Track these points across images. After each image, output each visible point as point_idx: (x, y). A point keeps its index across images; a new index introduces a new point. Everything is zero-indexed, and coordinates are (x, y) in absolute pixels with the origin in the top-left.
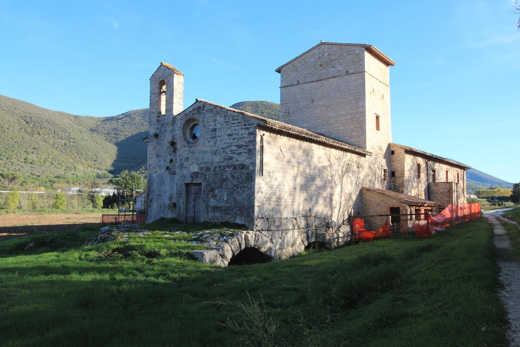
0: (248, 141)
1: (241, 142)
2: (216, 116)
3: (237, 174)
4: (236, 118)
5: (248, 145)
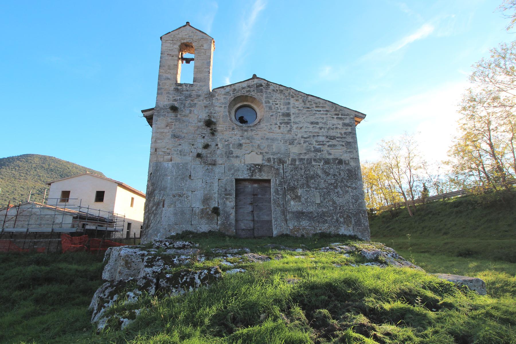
0: (343, 132)
1: (332, 133)
2: (289, 99)
5: (344, 138)
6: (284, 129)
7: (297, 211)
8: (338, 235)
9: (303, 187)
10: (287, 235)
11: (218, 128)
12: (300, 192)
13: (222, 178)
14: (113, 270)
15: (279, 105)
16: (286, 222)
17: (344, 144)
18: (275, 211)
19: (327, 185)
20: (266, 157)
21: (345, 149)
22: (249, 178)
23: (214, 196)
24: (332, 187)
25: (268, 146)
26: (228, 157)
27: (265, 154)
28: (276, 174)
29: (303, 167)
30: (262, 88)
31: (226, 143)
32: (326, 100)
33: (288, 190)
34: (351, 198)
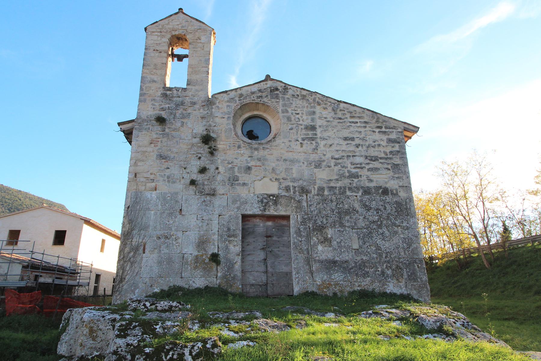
0: (388, 151)
1: (373, 152)
2: (314, 107)
3: (374, 203)
4: (357, 115)
5: (390, 158)
6: (308, 146)
7: (326, 260)
8: (385, 293)
9: (334, 225)
10: (313, 294)
11: (218, 146)
12: (330, 232)
13: (224, 213)
14: (72, 342)
15: (300, 114)
16: (312, 274)
17: (389, 167)
18: (297, 259)
19: (368, 223)
20: (283, 185)
21: (391, 173)
22: (260, 213)
23: (213, 238)
24: (375, 227)
25: (286, 170)
26: (232, 185)
27: (282, 181)
28: (296, 207)
29: (334, 198)
30: (278, 92)
31: (230, 166)
32: (364, 109)
33: (314, 230)
34: (401, 241)
